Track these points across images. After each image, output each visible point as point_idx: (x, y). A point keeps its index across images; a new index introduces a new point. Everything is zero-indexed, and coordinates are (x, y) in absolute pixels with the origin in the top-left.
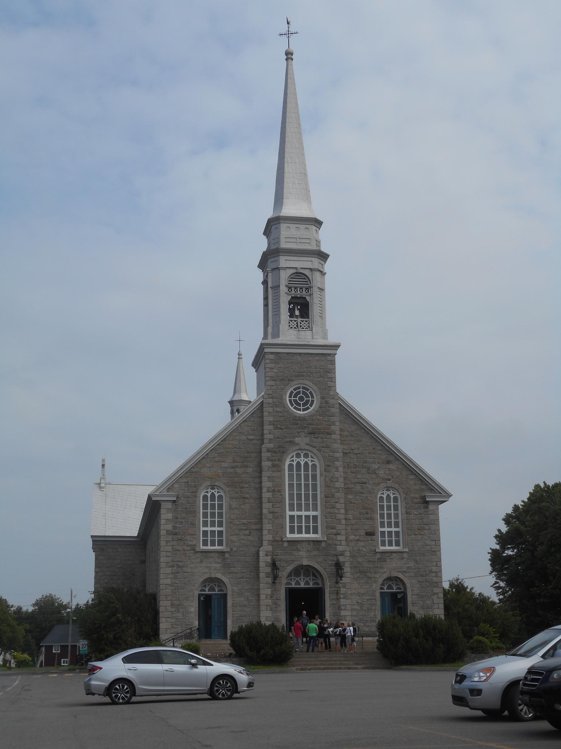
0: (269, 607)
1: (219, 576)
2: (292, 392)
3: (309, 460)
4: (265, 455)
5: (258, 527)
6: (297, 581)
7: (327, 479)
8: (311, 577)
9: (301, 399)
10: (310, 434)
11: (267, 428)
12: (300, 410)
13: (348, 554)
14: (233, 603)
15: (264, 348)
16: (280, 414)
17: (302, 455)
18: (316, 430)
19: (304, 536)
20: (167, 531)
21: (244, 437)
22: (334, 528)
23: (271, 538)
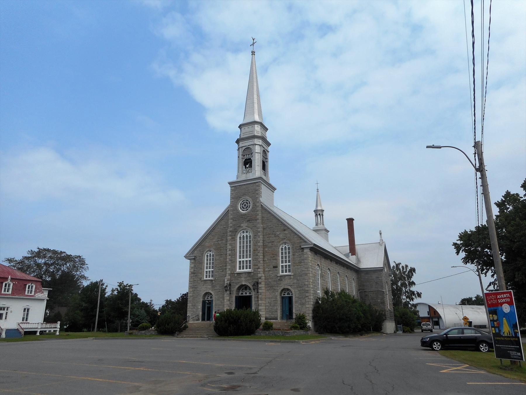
1: (210, 291)
3: (248, 234)
13: (263, 278)
18: (250, 219)
19: (245, 270)
21: (222, 227)
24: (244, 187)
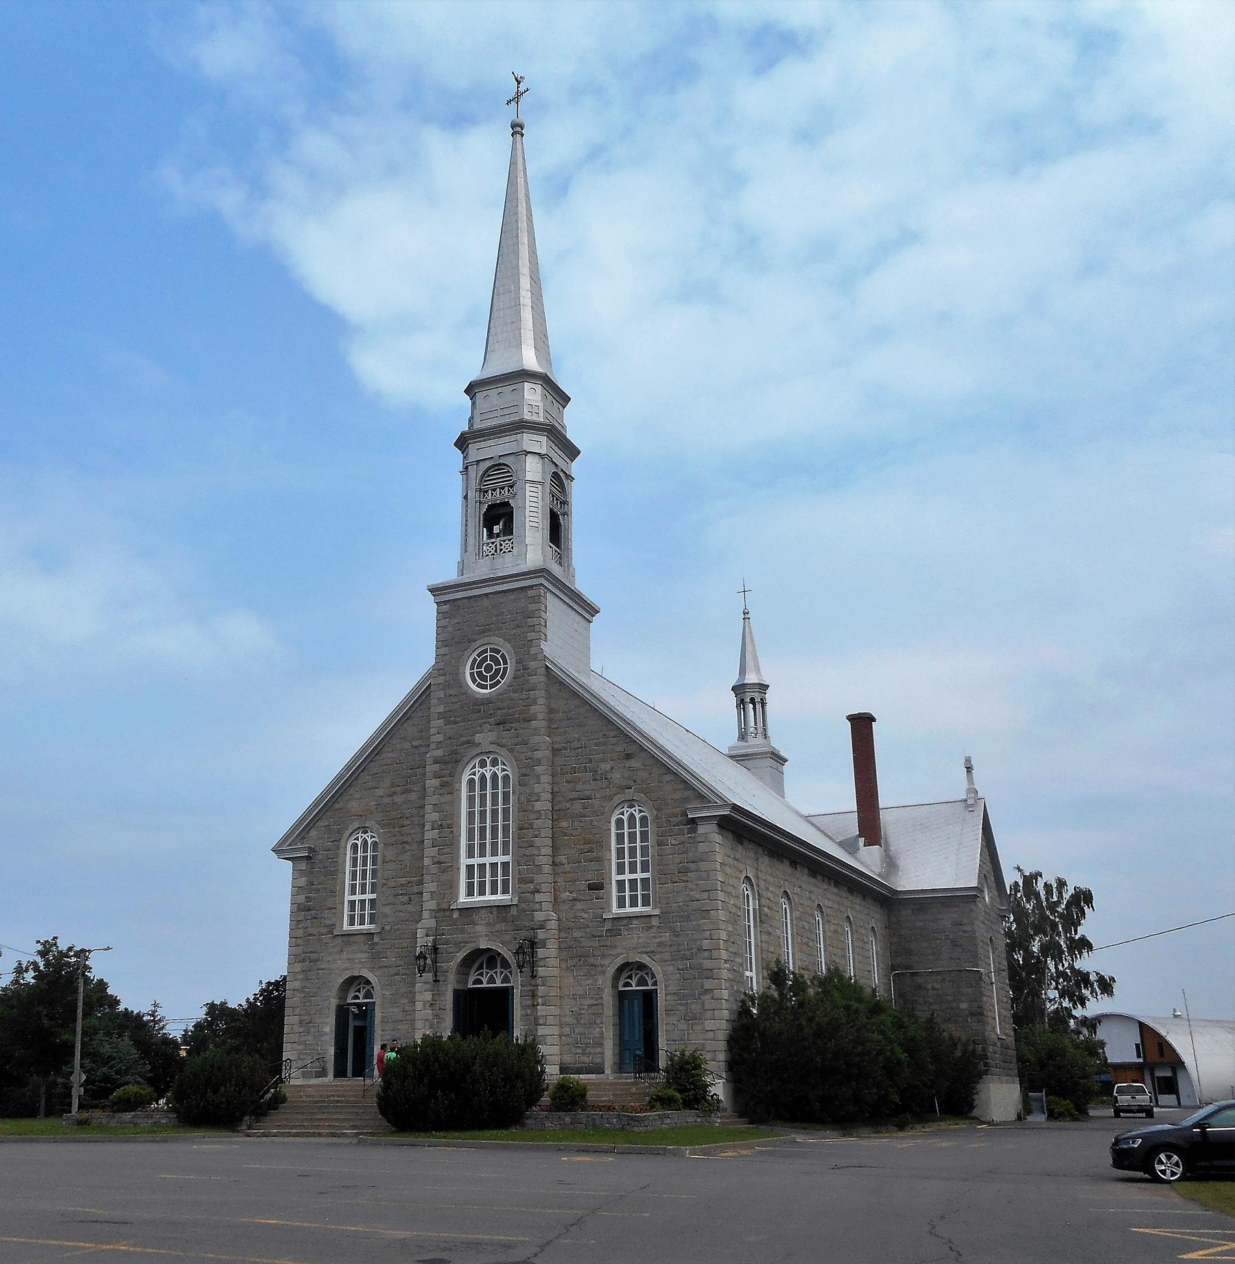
1: (365, 973)
3: (498, 770)
7: (522, 798)
13: (553, 924)
16: (455, 700)
18: (505, 717)
19: (488, 897)
21: (407, 745)
24: (486, 602)
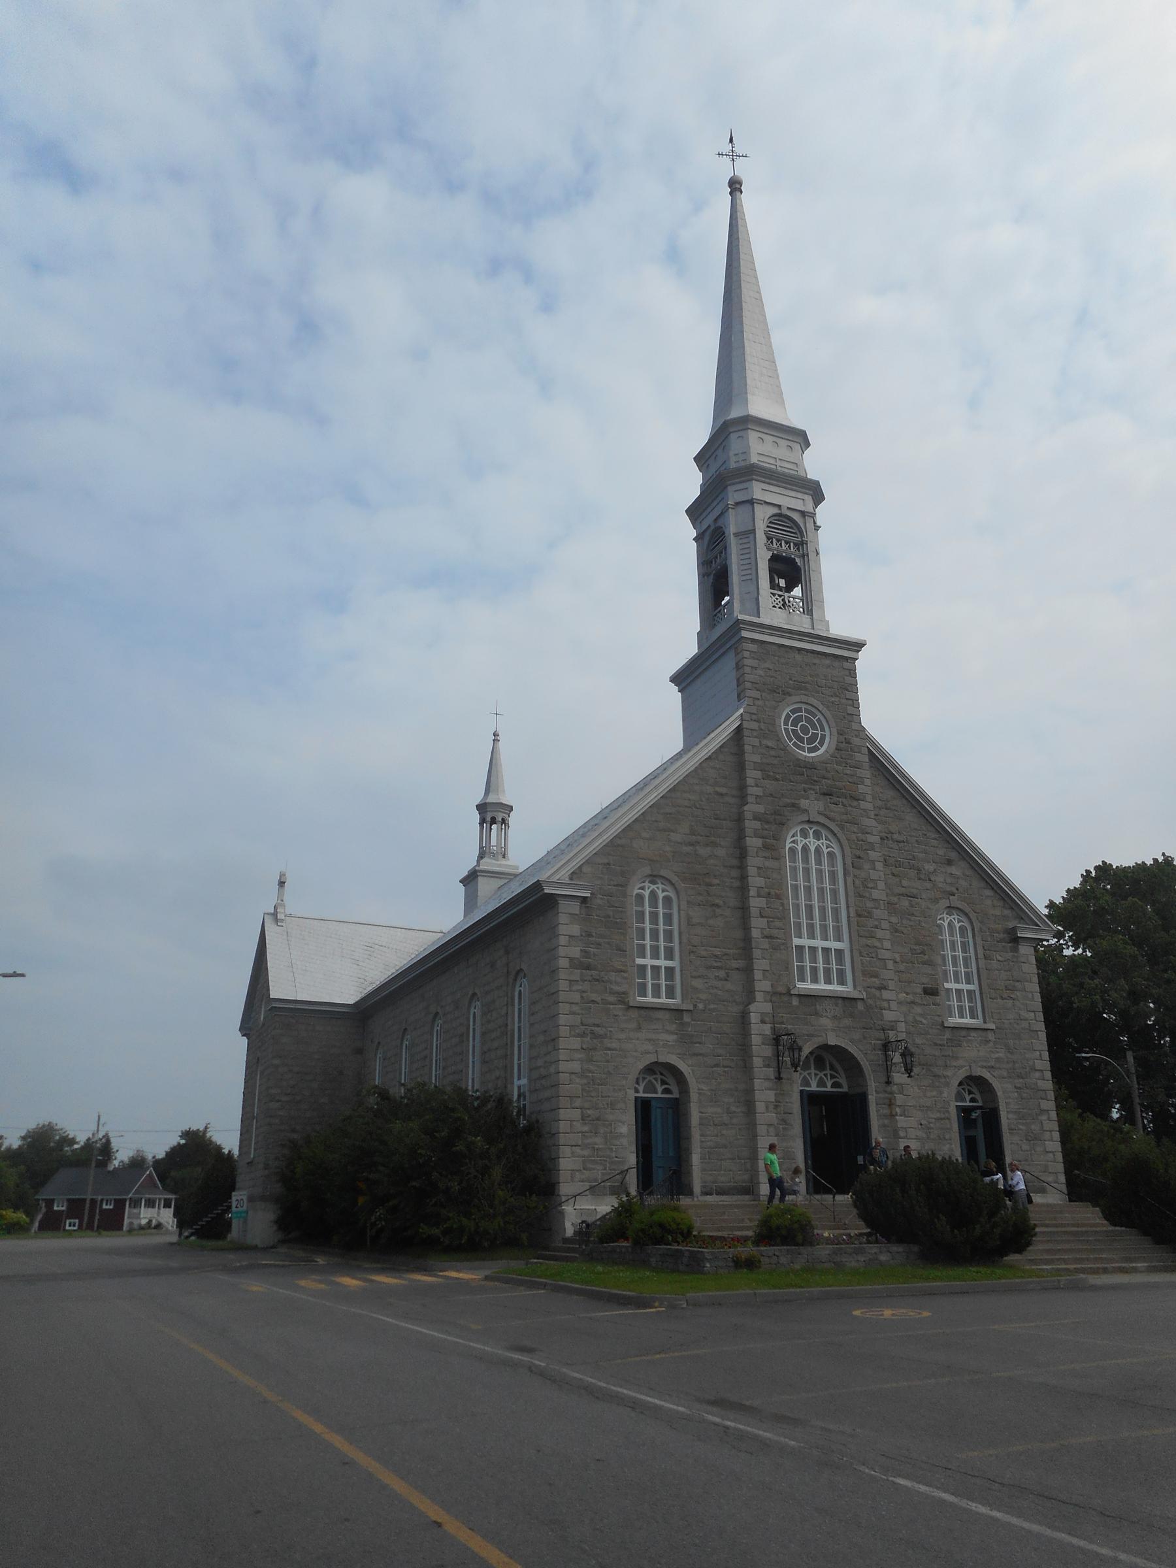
0: (771, 1129)
1: (673, 1060)
2: (788, 717)
4: (750, 825)
5: (741, 963)
6: (805, 1078)
7: (857, 882)
8: (828, 1072)
9: (805, 730)
10: (825, 794)
11: (752, 775)
12: (803, 749)
14: (701, 1118)
15: (740, 629)
16: (773, 753)
17: (811, 832)
19: (822, 987)
20: (571, 959)
21: (709, 789)
22: (876, 976)
23: (769, 989)
24: (798, 657)
